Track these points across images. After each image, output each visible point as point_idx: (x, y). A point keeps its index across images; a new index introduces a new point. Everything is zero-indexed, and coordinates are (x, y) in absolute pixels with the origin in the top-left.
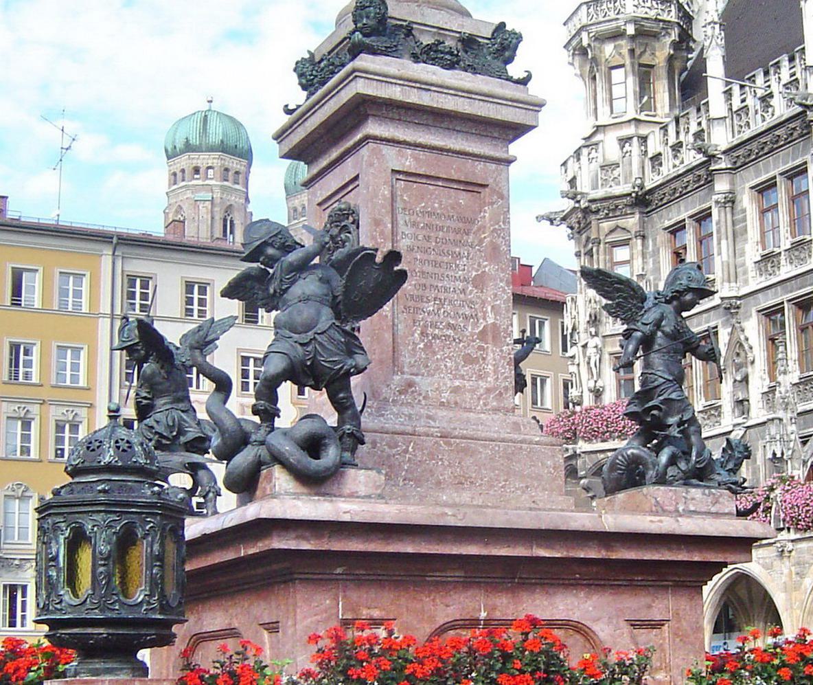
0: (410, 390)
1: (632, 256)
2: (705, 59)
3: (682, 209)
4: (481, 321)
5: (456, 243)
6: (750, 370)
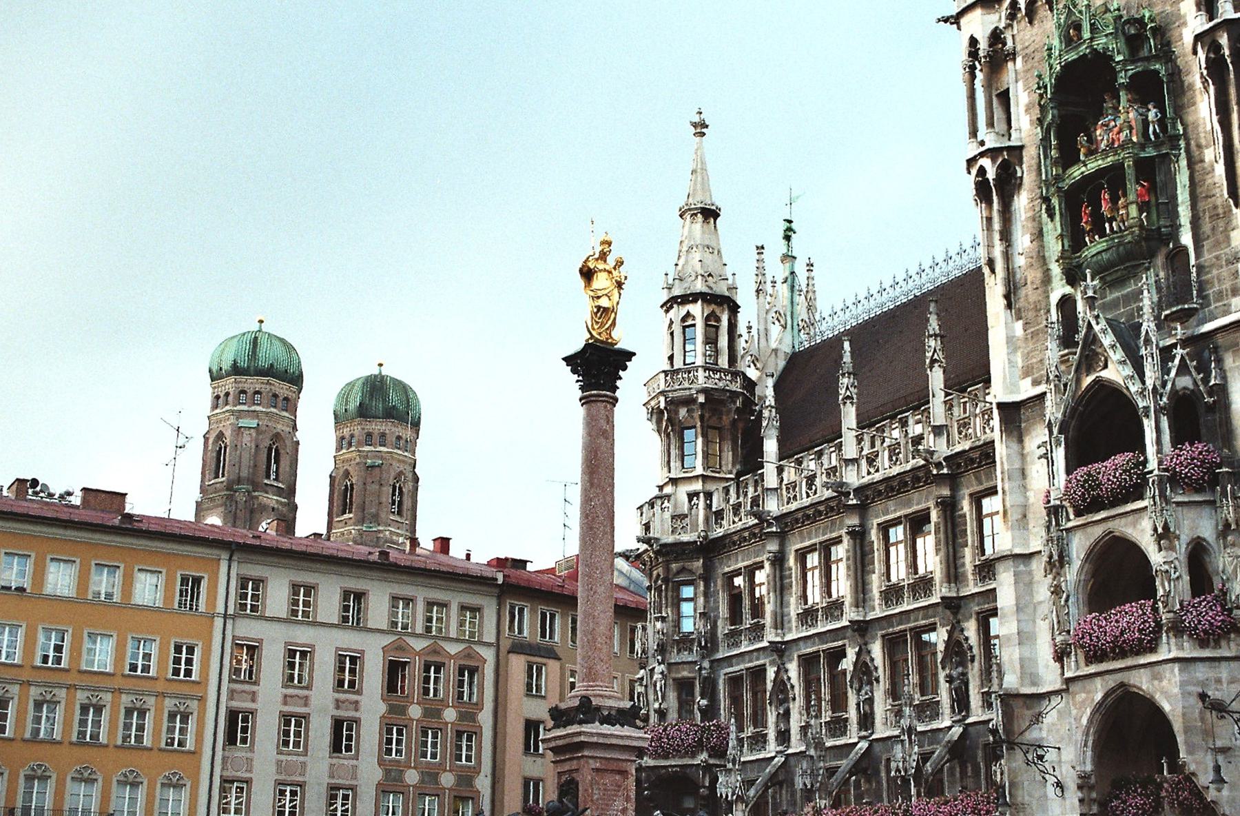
1: (695, 594)
2: (763, 438)
3: (740, 559)
6: (791, 706)
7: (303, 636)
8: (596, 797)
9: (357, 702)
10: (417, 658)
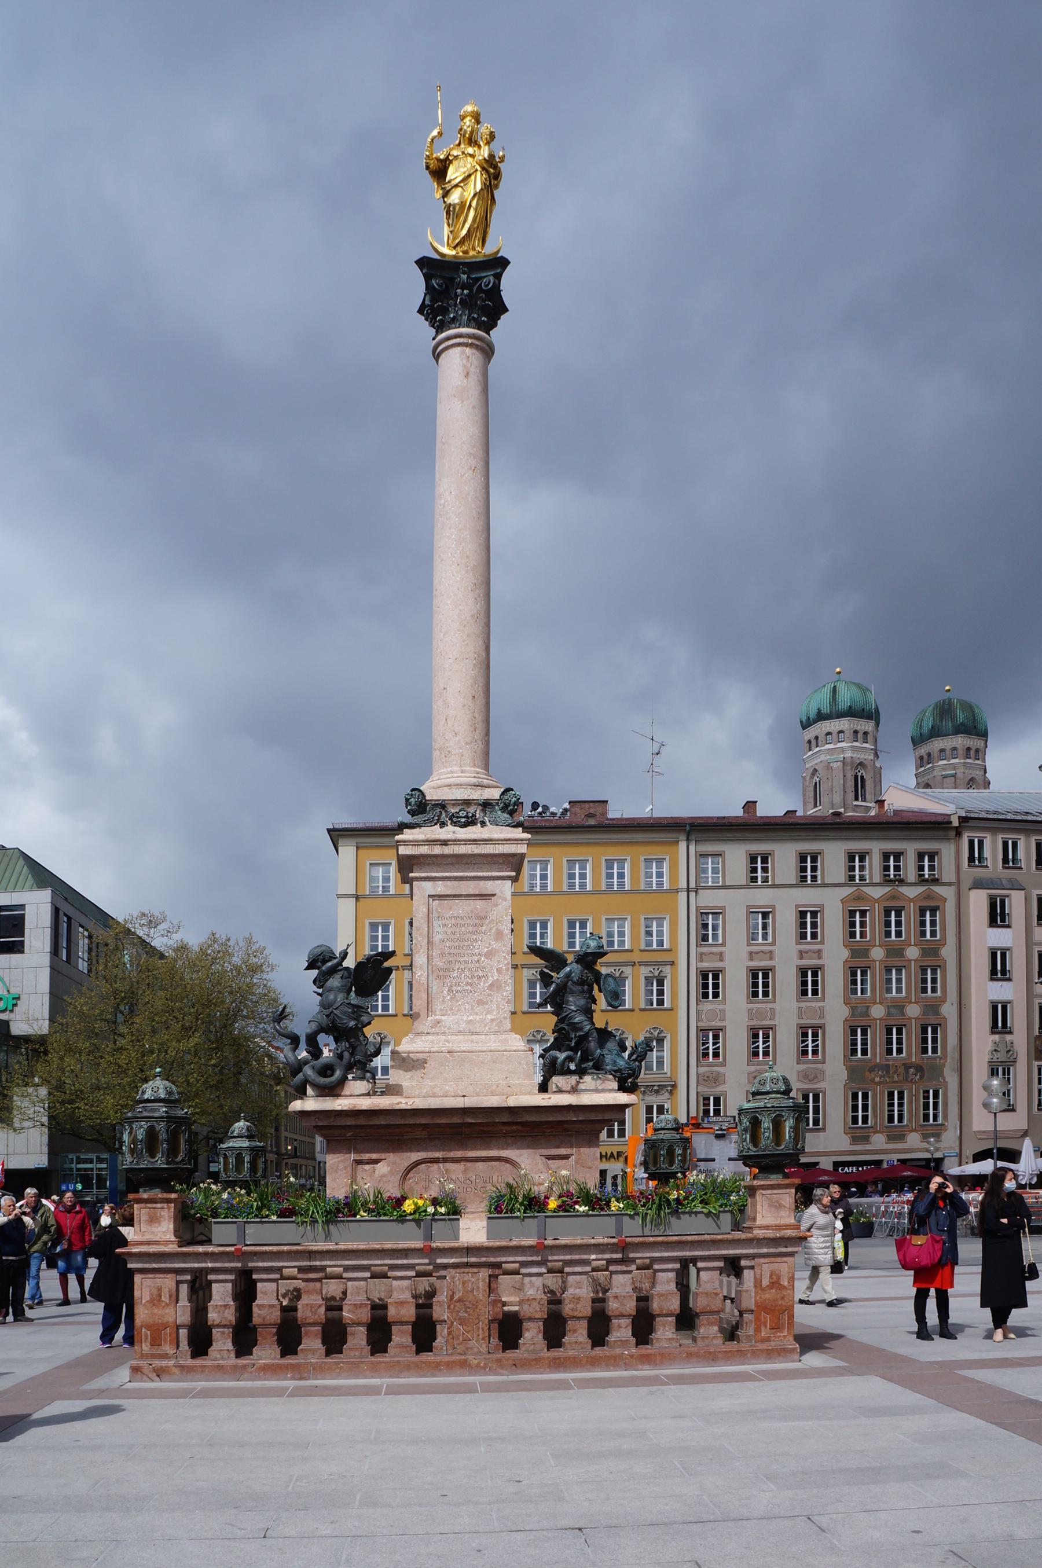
0: (439, 1025)
4: (490, 978)
5: (473, 933)
7: (762, 897)
8: (439, 937)
9: (820, 951)
10: (877, 904)
